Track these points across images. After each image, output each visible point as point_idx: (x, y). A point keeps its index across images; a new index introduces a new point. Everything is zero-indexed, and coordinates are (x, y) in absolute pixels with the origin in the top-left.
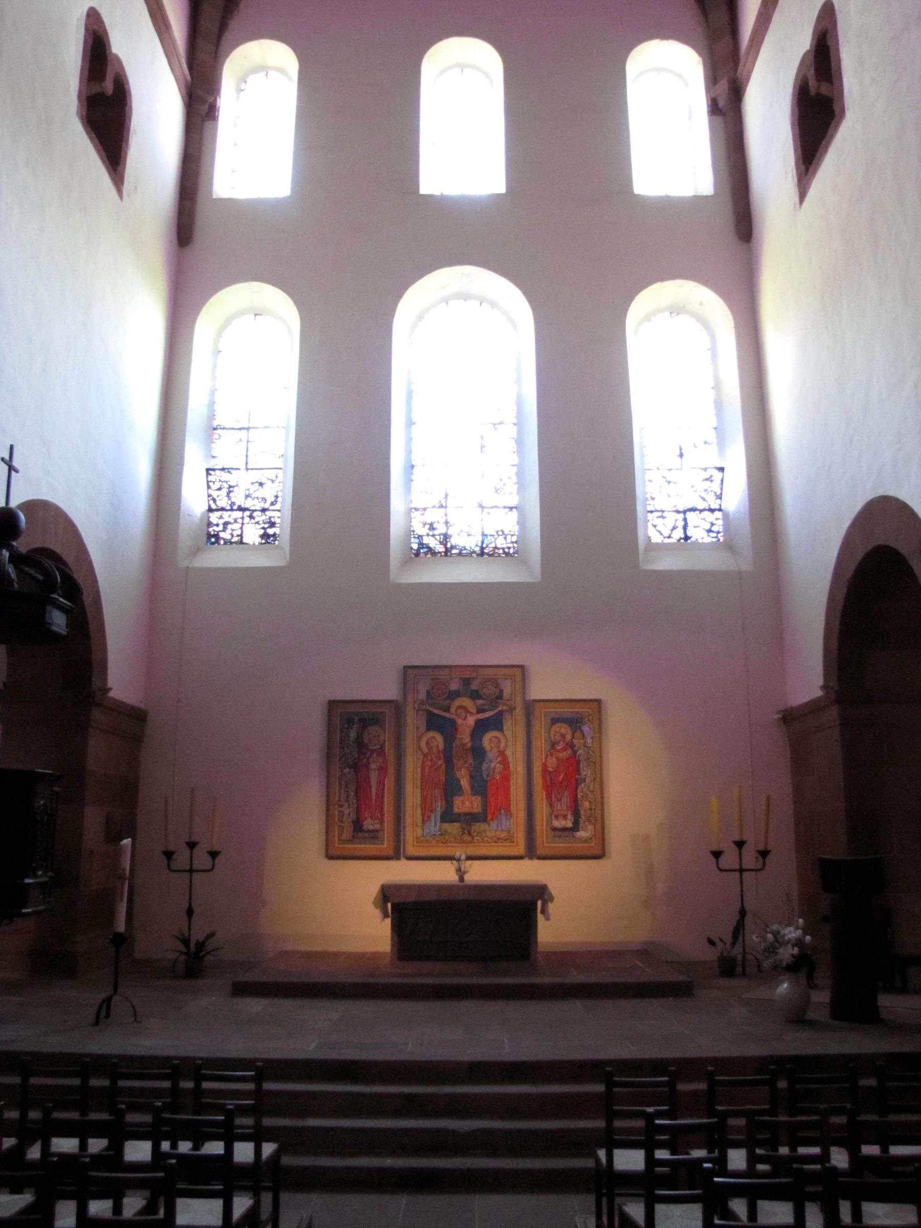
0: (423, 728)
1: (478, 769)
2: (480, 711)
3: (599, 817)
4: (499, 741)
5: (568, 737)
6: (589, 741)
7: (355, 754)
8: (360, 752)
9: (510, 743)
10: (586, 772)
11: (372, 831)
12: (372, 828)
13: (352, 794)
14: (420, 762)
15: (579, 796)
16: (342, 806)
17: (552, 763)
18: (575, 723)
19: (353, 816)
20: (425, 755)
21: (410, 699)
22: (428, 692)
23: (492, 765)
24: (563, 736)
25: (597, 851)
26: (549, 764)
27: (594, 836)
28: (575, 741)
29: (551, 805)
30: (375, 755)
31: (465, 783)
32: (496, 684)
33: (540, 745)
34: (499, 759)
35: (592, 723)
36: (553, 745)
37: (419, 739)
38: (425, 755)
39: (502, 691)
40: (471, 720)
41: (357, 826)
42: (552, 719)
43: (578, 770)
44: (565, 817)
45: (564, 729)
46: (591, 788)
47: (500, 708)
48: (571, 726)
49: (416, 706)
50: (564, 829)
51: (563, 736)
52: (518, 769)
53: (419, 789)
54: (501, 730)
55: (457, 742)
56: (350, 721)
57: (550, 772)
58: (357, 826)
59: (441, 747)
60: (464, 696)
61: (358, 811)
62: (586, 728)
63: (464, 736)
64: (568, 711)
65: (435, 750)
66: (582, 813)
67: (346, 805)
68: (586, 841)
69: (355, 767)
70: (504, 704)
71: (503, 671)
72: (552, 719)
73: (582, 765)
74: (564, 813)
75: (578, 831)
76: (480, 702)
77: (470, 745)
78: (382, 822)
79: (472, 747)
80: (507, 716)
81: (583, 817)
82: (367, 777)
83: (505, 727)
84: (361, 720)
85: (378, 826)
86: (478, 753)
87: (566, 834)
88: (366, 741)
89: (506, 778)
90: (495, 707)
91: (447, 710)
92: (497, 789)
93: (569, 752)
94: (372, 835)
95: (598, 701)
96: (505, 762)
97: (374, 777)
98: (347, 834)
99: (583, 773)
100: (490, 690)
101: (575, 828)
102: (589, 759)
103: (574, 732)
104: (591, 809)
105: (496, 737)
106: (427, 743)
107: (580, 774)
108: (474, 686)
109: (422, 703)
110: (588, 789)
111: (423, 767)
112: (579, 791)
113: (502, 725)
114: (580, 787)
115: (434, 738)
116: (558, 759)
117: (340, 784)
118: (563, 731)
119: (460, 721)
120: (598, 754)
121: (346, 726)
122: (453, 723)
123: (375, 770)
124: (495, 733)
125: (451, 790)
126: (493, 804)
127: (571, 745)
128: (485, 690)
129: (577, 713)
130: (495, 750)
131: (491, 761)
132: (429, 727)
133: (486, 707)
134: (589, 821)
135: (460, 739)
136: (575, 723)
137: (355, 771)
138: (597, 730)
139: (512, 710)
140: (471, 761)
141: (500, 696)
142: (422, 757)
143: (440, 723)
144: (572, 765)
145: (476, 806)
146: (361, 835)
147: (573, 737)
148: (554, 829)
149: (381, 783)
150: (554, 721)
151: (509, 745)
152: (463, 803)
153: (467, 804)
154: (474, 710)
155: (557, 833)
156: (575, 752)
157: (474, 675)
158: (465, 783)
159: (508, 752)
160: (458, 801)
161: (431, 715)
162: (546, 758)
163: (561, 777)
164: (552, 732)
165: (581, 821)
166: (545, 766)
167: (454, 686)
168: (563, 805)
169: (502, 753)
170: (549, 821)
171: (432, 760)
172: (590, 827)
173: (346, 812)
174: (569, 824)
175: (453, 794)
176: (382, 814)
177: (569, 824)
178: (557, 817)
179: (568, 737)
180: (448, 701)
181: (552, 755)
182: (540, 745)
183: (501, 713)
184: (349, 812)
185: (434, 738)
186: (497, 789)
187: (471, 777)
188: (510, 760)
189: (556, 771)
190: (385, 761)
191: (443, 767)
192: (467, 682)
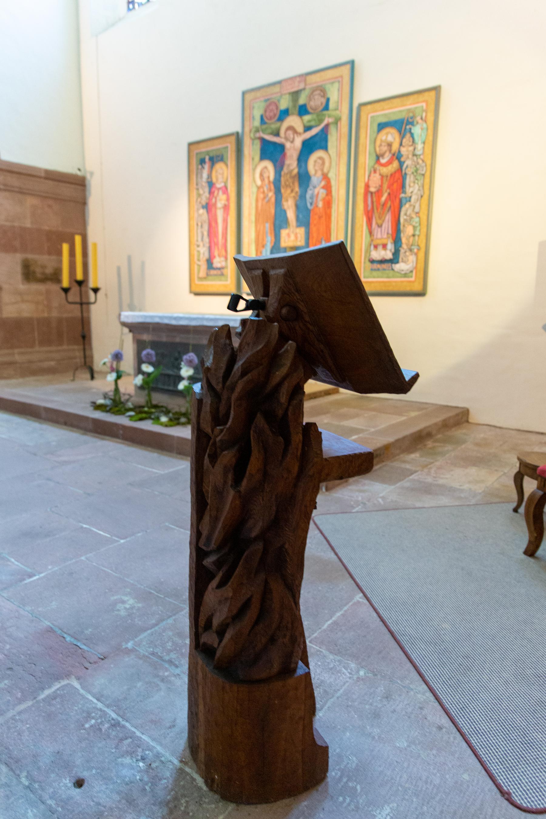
0: (257, 158)
1: (303, 196)
2: (307, 128)
3: (423, 245)
4: (323, 163)
5: (395, 147)
6: (420, 146)
7: (207, 194)
8: (211, 193)
9: (334, 164)
10: (412, 188)
11: (219, 269)
12: (219, 265)
13: (206, 234)
14: (255, 196)
15: (402, 220)
16: (198, 246)
17: (375, 183)
18: (403, 126)
19: (207, 255)
20: (259, 188)
21: (247, 129)
22: (262, 117)
23: (316, 191)
24: (390, 145)
25: (417, 287)
26: (371, 183)
27: (416, 268)
28: (403, 150)
29: (371, 233)
30: (221, 192)
31: (291, 215)
32: (323, 91)
33: (366, 160)
34: (323, 183)
35: (426, 122)
36: (378, 157)
37: (254, 170)
38: (259, 188)
39: (328, 100)
40: (298, 142)
41: (210, 263)
42: (379, 125)
43: (403, 186)
44: (384, 246)
45: (391, 136)
46: (417, 209)
47: (325, 122)
48: (400, 131)
49: (252, 135)
50: (383, 261)
51: (390, 145)
52: (339, 192)
53: (253, 225)
54: (325, 148)
55: (285, 170)
56: (202, 162)
57: (372, 193)
58: (210, 263)
59: (272, 178)
60: (293, 114)
61: (210, 249)
62: (417, 130)
63: (291, 163)
64: (396, 111)
65: (266, 181)
66: (404, 240)
67: (201, 244)
68: (405, 275)
69: (209, 207)
70: (329, 116)
71: (330, 74)
72: (379, 125)
73: (409, 180)
74: (384, 241)
75: (398, 262)
76: (307, 118)
77: (296, 171)
78: (226, 258)
79: (299, 173)
80: (332, 131)
81: (404, 246)
82: (216, 215)
83: (330, 144)
84: (212, 159)
85: (223, 264)
86: (304, 178)
87: (385, 266)
88: (214, 180)
89: (328, 204)
90: (321, 121)
91: (277, 134)
92: (320, 217)
93: (395, 164)
94: (219, 272)
95: (437, 89)
96: (328, 187)
97: (220, 214)
98: (203, 274)
99: (409, 190)
100: (317, 102)
101: (395, 260)
102: (416, 171)
103: (402, 137)
104: (414, 235)
105: (320, 158)
106: (261, 175)
107: (405, 192)
108: (302, 101)
109: (257, 130)
110: (413, 211)
111: (257, 200)
112: (402, 213)
113: (326, 141)
114: (403, 210)
115: (266, 168)
116: (382, 177)
117: (197, 225)
118: (390, 138)
119: (288, 145)
120: (429, 162)
121: (200, 167)
122: (282, 147)
123: (220, 209)
124: (320, 153)
125: (279, 222)
126: (315, 235)
127: (398, 156)
128: (312, 103)
129: (409, 111)
130: (319, 173)
131: (315, 187)
132: (262, 158)
133: (313, 123)
134: (411, 250)
135: (289, 165)
136: (403, 126)
137: (208, 212)
138: (431, 132)
139: (337, 120)
140: (297, 189)
141: (326, 108)
142: (255, 190)
143: (272, 151)
144: (398, 180)
145: (299, 239)
146: (212, 272)
147: (401, 144)
148: (372, 261)
149: (225, 221)
150: (382, 127)
151: (331, 165)
152: (289, 235)
153: (292, 237)
154: (300, 129)
155: (376, 266)
156: (401, 164)
157: (302, 86)
158: (291, 215)
159: (331, 175)
160: (284, 233)
161: (263, 141)
162: (369, 176)
163: (383, 199)
164: (378, 143)
165: (402, 251)
166: (367, 186)
167: (284, 104)
168: (383, 233)
169: (325, 177)
170: (368, 251)
171: (264, 192)
172: (412, 258)
173: (202, 251)
174: (388, 255)
175: (281, 228)
176: (226, 251)
177: (388, 255)
178: (376, 247)
179: (395, 147)
180: (278, 124)
181: (375, 172)
182: (366, 160)
183: (327, 126)
184: (204, 251)
185: (266, 168)
186: (320, 217)
187: (297, 206)
188: (333, 183)
189: (379, 192)
190: (228, 199)
191: (273, 199)
192: (295, 95)
